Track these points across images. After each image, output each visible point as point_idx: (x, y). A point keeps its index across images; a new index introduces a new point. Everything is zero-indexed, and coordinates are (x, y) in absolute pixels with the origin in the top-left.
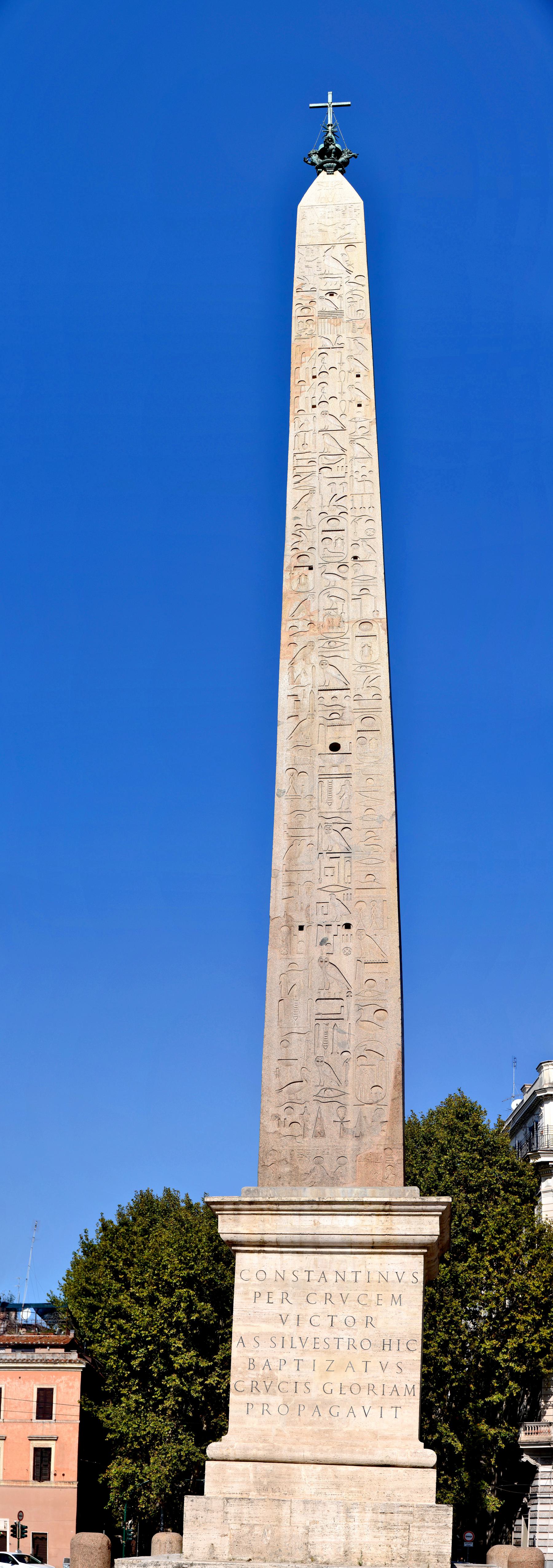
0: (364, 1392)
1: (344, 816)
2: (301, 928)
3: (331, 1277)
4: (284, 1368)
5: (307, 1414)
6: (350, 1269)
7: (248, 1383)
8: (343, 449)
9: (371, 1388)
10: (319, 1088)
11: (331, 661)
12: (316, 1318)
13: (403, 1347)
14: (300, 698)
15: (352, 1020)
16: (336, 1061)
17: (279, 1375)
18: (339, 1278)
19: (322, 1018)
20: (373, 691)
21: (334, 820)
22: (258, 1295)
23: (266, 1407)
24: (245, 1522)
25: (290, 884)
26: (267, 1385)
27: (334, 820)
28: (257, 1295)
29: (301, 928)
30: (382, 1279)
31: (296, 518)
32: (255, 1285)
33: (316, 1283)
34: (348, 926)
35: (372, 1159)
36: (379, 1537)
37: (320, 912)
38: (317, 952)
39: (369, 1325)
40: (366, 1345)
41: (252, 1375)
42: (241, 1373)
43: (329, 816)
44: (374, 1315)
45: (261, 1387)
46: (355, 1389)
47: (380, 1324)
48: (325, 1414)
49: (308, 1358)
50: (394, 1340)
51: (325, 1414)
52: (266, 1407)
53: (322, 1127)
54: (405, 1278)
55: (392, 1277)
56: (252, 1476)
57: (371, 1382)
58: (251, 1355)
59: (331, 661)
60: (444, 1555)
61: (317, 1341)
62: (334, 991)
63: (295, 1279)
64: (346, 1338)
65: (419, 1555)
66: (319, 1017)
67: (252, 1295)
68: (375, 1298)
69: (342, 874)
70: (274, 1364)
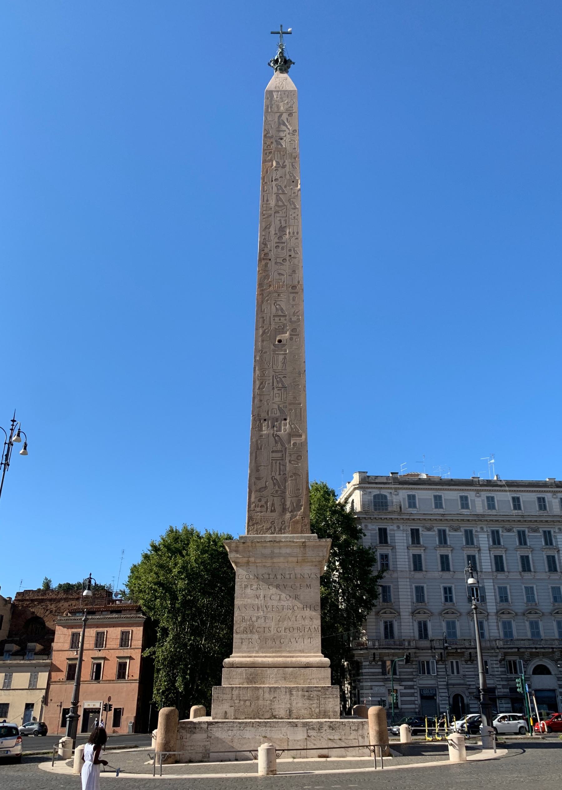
0: (296, 631)
2: (265, 420)
3: (279, 577)
4: (259, 620)
5: (269, 643)
6: (287, 573)
7: (242, 629)
9: (298, 629)
10: (273, 490)
11: (278, 303)
12: (273, 596)
13: (312, 608)
15: (287, 461)
17: (255, 624)
18: (282, 577)
21: (279, 373)
22: (246, 586)
23: (250, 640)
24: (241, 699)
26: (251, 629)
27: (279, 373)
28: (246, 586)
30: (302, 577)
32: (245, 582)
33: (272, 579)
35: (297, 522)
36: (306, 704)
37: (273, 413)
39: (297, 599)
40: (296, 608)
41: (244, 625)
42: (239, 624)
43: (277, 371)
44: (299, 594)
45: (248, 630)
46: (291, 629)
47: (302, 598)
48: (278, 642)
49: (270, 615)
50: (308, 605)
51: (278, 642)
52: (250, 640)
53: (274, 508)
54: (312, 576)
55: (306, 576)
56: (244, 675)
57: (298, 626)
58: (243, 615)
60: (336, 712)
61: (274, 607)
63: (263, 578)
64: (286, 605)
65: (325, 712)
66: (273, 459)
67: (244, 586)
68: (299, 586)
69: (283, 397)
70: (254, 619)
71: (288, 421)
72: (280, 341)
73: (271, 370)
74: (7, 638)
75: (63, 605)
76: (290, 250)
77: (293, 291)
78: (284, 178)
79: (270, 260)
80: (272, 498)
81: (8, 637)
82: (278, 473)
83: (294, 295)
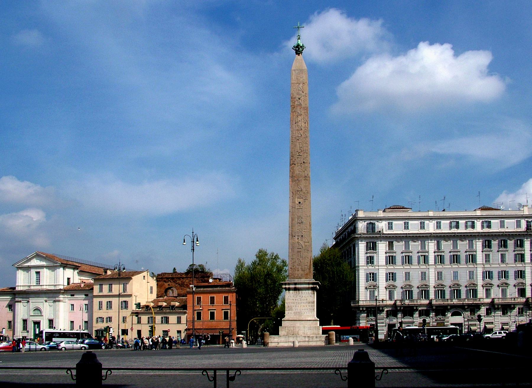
1: (301, 216)
8: (301, 135)
11: (299, 185)
14: (293, 193)
16: (301, 259)
19: (298, 252)
20: (307, 191)
25: (292, 228)
29: (294, 236)
31: (292, 152)
34: (302, 236)
38: (297, 240)
59: (299, 185)
62: (300, 247)
71: (303, 237)
72: (300, 203)
73: (296, 215)
74: (156, 298)
75: (185, 281)
76: (304, 159)
77: (305, 179)
78: (301, 122)
79: (295, 164)
80: (297, 266)
81: (157, 298)
82: (300, 257)
83: (306, 181)
